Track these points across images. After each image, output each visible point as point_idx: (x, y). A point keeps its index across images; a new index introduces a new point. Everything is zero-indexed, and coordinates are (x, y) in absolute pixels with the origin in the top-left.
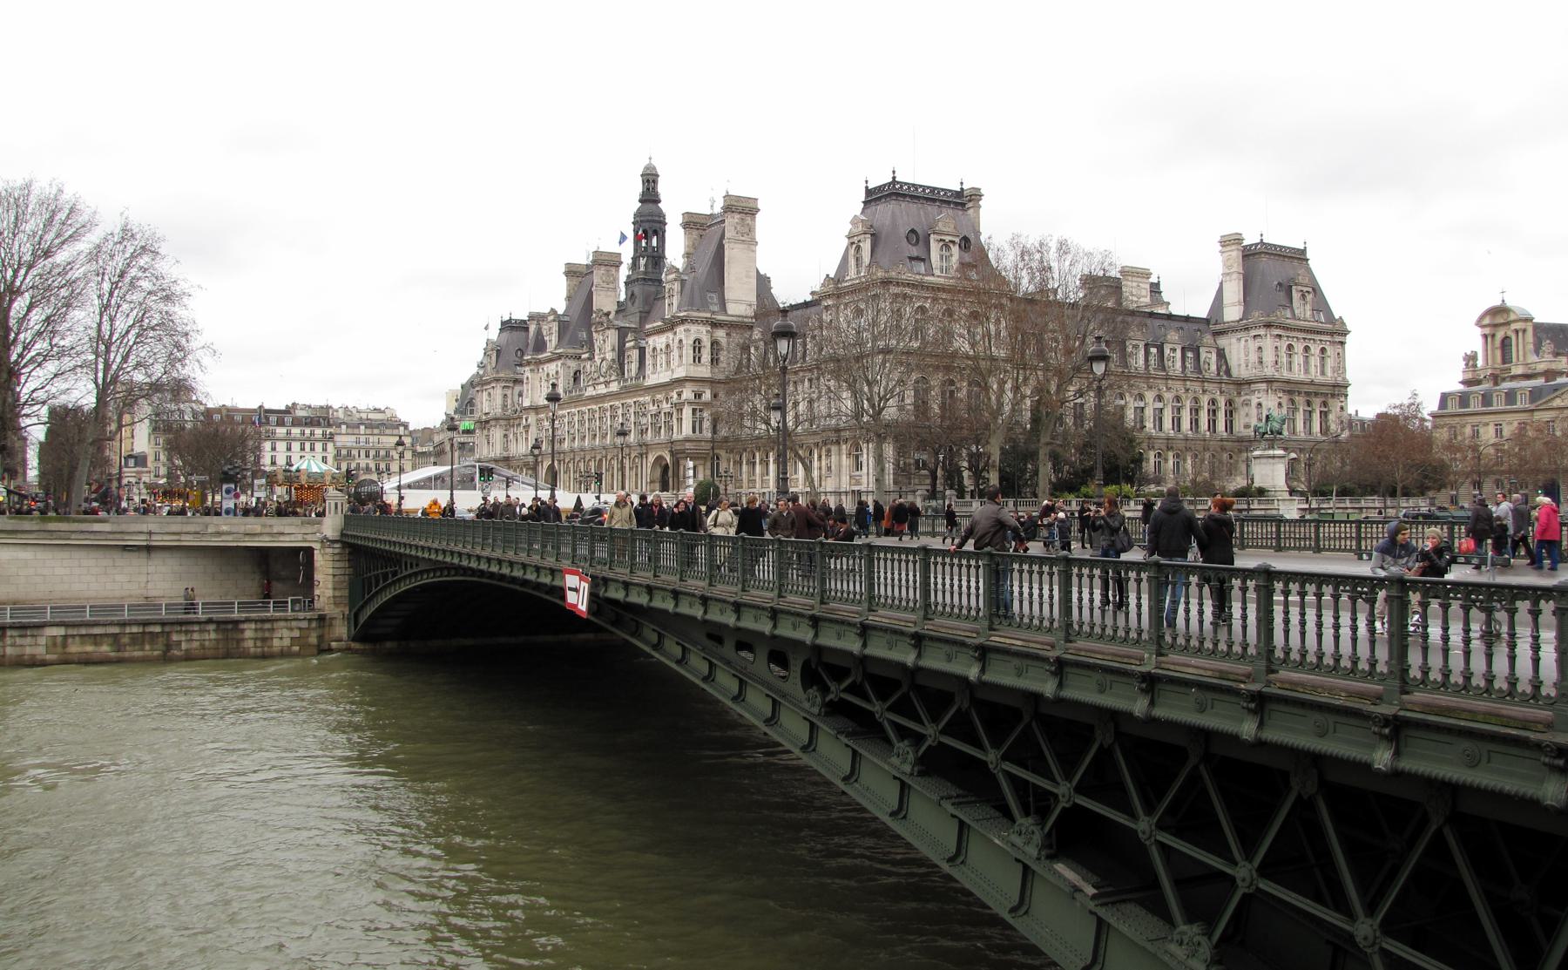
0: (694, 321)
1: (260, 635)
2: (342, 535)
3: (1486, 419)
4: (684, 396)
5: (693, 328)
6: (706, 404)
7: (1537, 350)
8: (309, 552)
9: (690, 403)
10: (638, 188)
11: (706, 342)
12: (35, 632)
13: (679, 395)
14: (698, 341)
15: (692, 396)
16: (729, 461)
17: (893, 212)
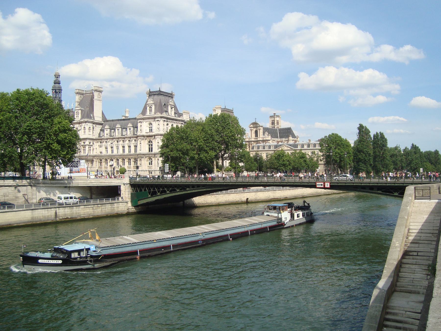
0: (89, 122)
1: (117, 206)
2: (130, 182)
3: (263, 152)
4: (86, 144)
5: (89, 124)
6: (92, 146)
7: (264, 134)
8: (120, 186)
9: (88, 145)
10: (54, 79)
11: (92, 128)
12: (79, 207)
13: (84, 143)
14: (90, 128)
15: (88, 143)
16: (96, 161)
17: (160, 99)
